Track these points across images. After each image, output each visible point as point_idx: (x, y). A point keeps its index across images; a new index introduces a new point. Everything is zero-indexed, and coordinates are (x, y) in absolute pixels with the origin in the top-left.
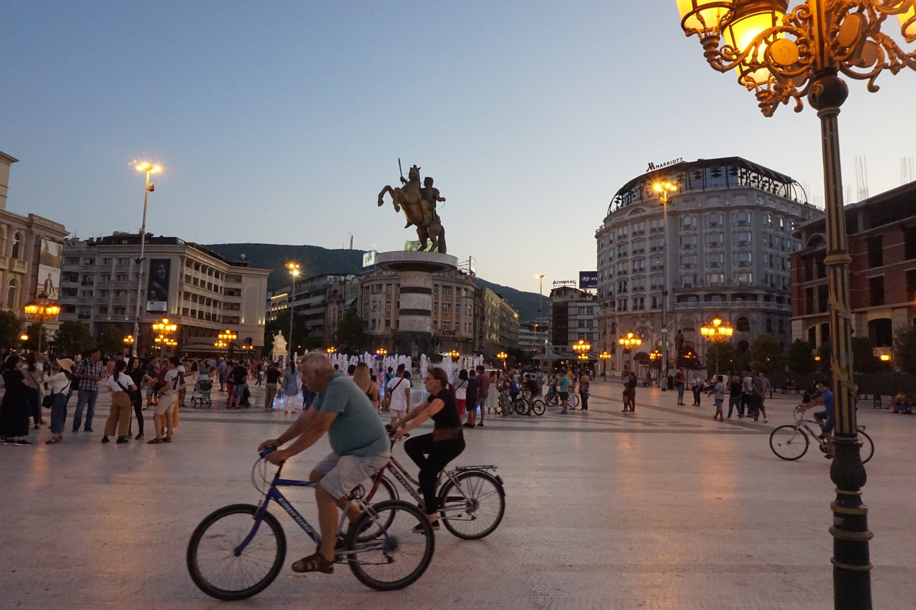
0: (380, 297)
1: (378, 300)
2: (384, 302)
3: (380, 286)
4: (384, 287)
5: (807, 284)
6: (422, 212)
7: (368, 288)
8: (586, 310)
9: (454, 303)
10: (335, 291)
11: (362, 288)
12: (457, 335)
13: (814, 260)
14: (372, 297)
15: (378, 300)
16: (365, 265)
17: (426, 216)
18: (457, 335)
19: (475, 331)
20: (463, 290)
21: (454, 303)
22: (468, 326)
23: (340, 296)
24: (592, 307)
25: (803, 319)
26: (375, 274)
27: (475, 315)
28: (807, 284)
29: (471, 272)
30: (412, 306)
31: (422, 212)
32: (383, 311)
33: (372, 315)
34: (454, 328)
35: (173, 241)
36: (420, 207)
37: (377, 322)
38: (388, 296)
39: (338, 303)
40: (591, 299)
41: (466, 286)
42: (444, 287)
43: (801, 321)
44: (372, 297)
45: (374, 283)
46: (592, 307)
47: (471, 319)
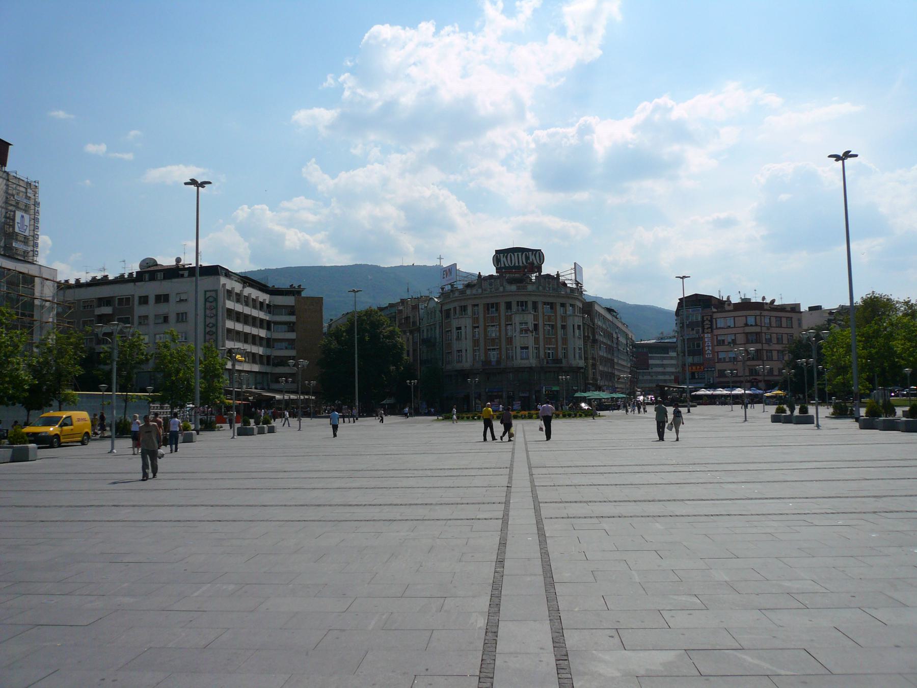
0: (466, 322)
2: (469, 329)
3: (464, 309)
7: (448, 311)
9: (559, 326)
10: (407, 318)
11: (441, 311)
12: (564, 363)
14: (455, 323)
18: (564, 363)
19: (586, 359)
20: (568, 305)
21: (559, 326)
22: (577, 351)
23: (414, 323)
26: (457, 294)
27: (584, 336)
29: (577, 283)
33: (456, 346)
34: (560, 355)
35: (214, 271)
37: (464, 353)
38: (475, 320)
39: (411, 332)
40: (731, 308)
41: (572, 302)
42: (545, 303)
45: (456, 304)
47: (580, 343)
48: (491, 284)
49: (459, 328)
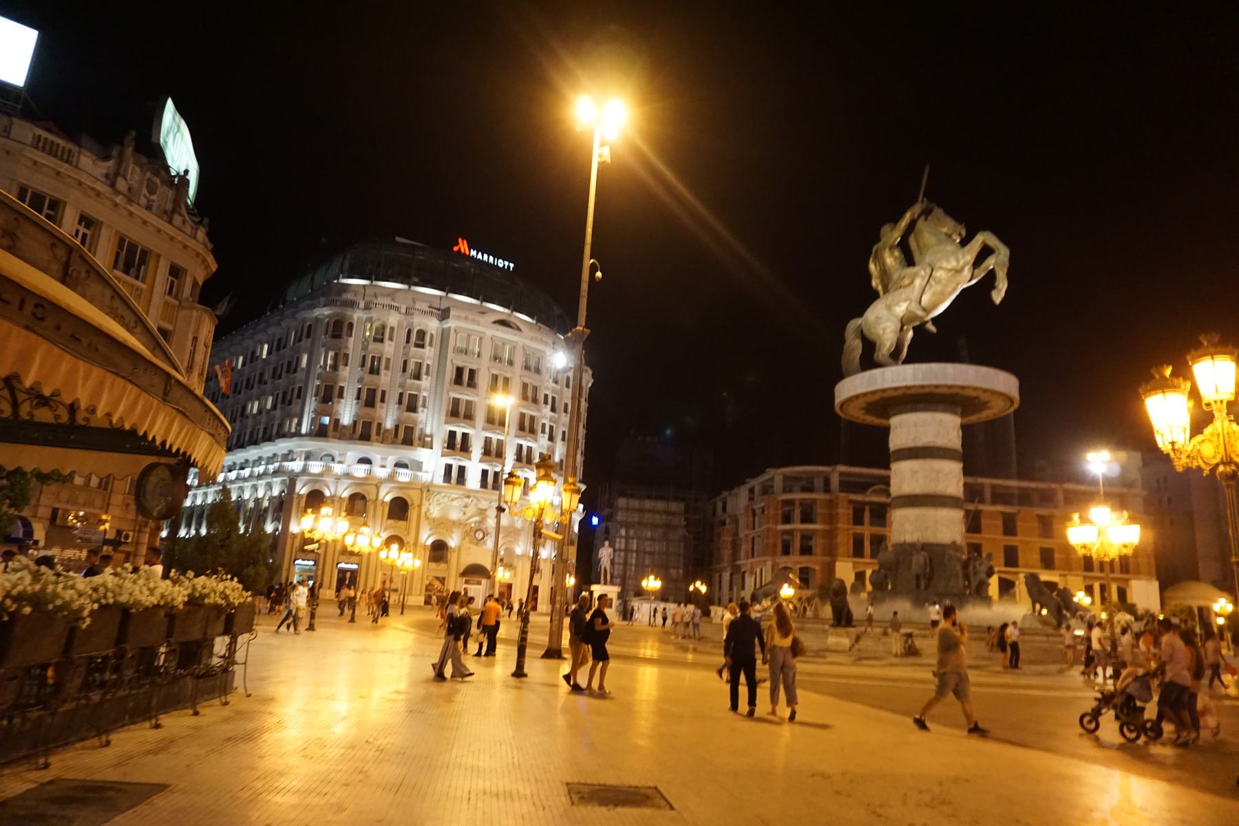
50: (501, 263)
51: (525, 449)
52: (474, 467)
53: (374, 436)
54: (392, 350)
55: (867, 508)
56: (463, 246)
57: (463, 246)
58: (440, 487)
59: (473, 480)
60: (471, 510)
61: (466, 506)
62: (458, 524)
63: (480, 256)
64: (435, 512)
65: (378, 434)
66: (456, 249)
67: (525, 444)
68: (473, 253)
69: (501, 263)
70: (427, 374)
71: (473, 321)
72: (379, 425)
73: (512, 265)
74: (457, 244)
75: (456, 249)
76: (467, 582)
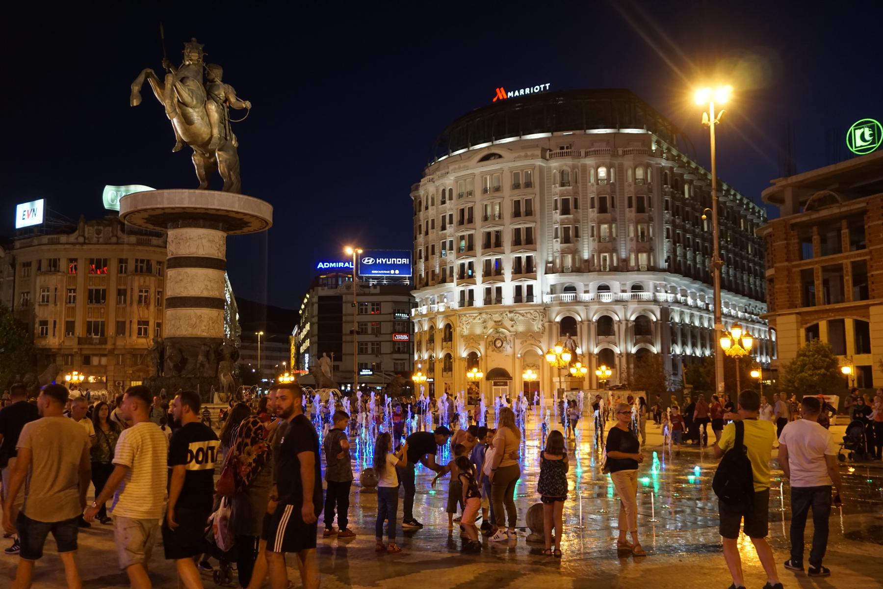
1: (52, 288)
2: (63, 294)
3: (54, 264)
4: (63, 265)
5: (806, 264)
6: (210, 125)
7: (27, 265)
8: (370, 307)
11: (13, 265)
13: (815, 229)
15: (52, 288)
16: (20, 223)
17: (216, 132)
24: (379, 304)
25: (797, 313)
28: (806, 264)
30: (195, 290)
31: (210, 125)
32: (62, 307)
33: (41, 313)
36: (208, 115)
37: (50, 326)
43: (793, 318)
44: (40, 280)
46: (379, 304)
48: (98, 232)
49: (45, 289)
50: (537, 89)
51: (524, 261)
52: (479, 289)
53: (430, 283)
54: (434, 212)
55: (844, 223)
56: (501, 94)
57: (501, 94)
58: (460, 311)
59: (479, 300)
60: (490, 324)
61: (484, 322)
62: (480, 337)
63: (517, 93)
64: (466, 332)
65: (433, 279)
66: (495, 99)
67: (524, 256)
68: (510, 94)
69: (537, 89)
70: (451, 222)
71: (467, 168)
72: (433, 272)
73: (547, 85)
74: (496, 94)
75: (495, 99)
76: (495, 384)
